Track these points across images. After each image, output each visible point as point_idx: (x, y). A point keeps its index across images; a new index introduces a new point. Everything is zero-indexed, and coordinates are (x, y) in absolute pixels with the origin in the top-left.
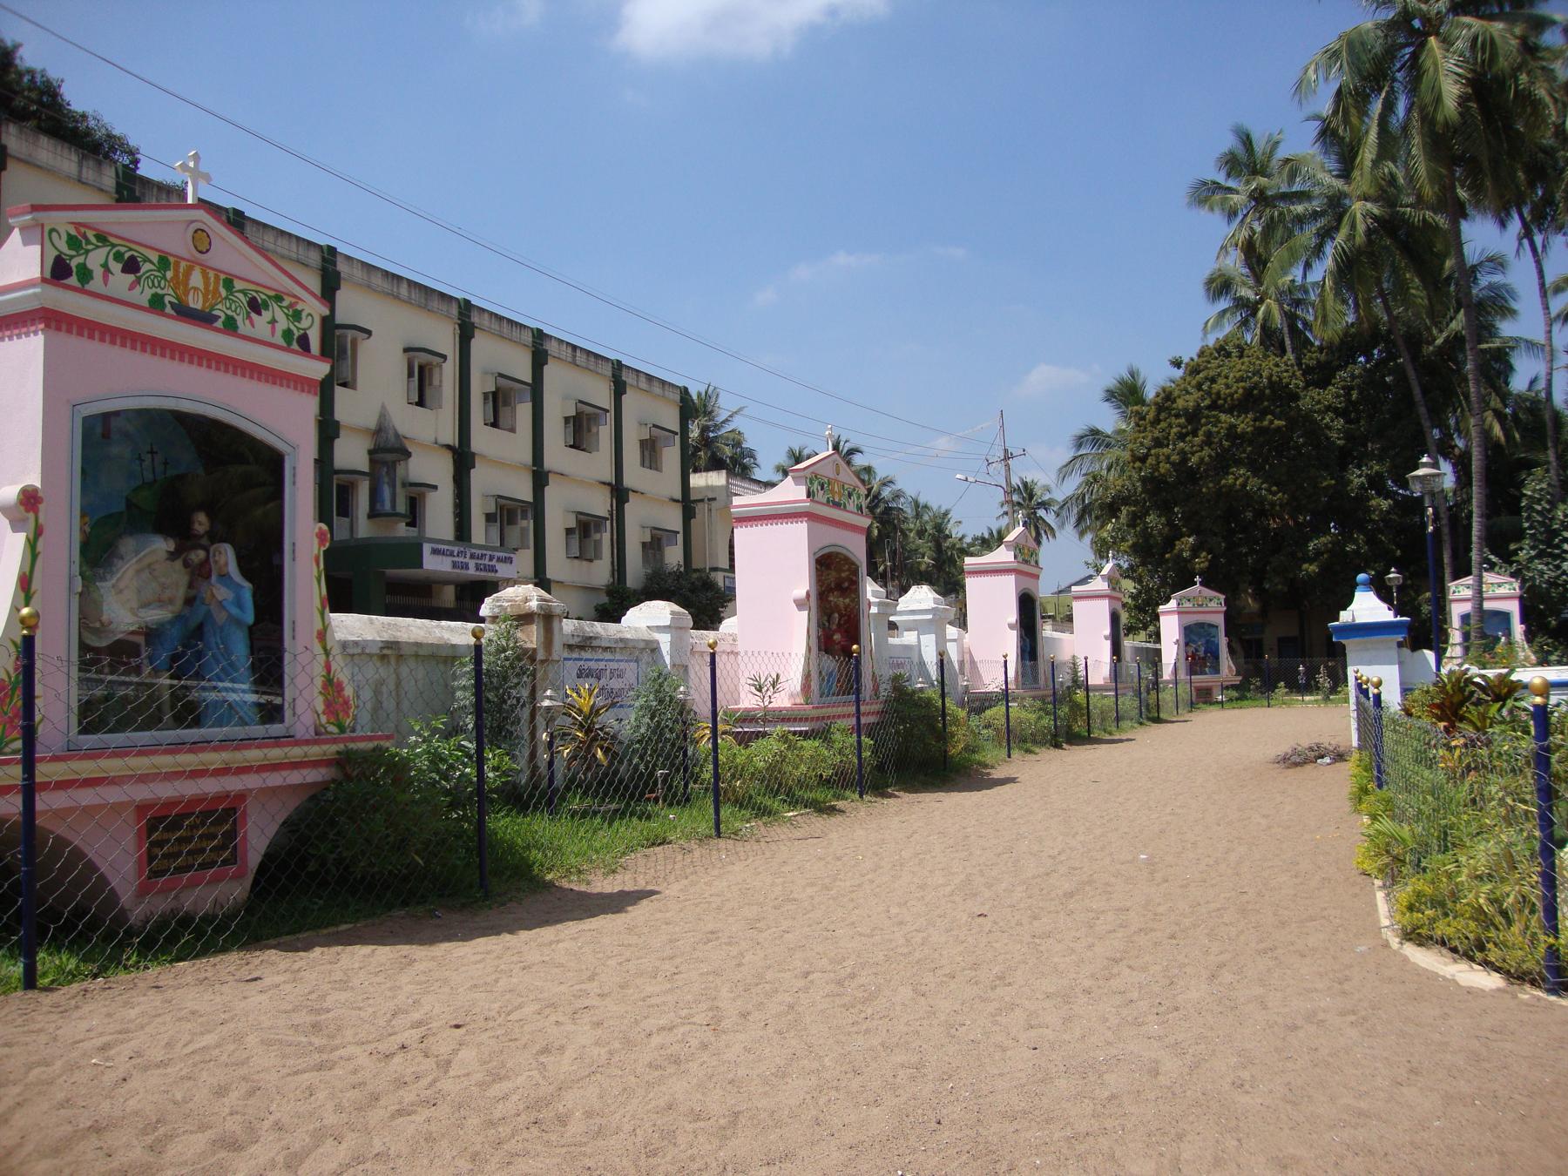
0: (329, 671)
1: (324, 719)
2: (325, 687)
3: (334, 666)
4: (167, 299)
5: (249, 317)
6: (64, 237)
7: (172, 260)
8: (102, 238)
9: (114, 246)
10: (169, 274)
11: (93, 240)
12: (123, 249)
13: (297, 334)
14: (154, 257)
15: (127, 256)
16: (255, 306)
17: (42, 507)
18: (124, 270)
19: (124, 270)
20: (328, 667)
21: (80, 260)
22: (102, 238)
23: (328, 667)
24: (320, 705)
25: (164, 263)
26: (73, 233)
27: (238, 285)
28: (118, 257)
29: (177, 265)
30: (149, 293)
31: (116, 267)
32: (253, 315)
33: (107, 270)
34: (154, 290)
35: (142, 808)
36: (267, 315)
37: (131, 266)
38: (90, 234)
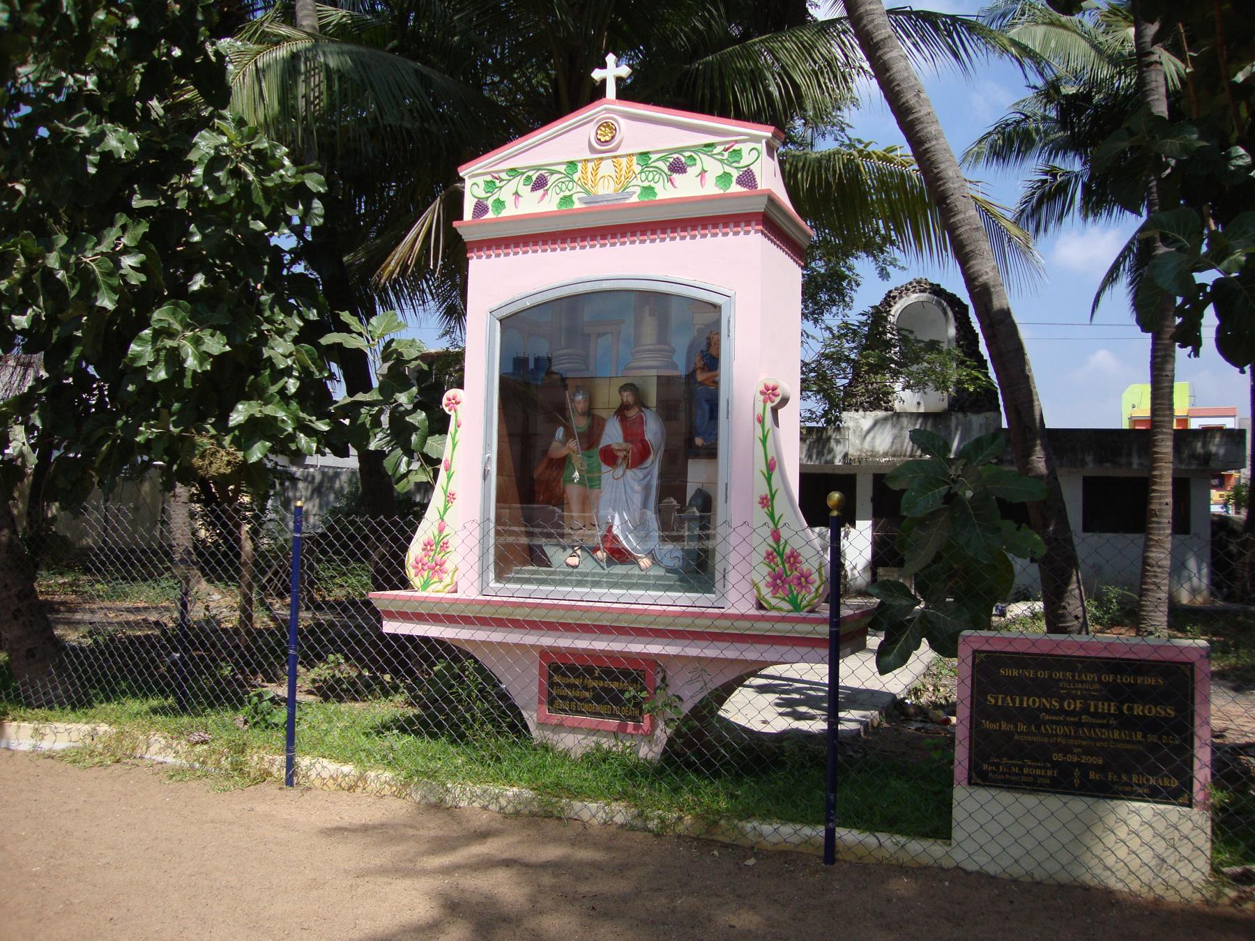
1: (766, 592)
2: (770, 557)
3: (784, 533)
4: (575, 198)
5: (670, 180)
6: (482, 185)
8: (514, 172)
10: (576, 177)
12: (530, 173)
13: (735, 174)
15: (534, 178)
16: (677, 168)
19: (534, 189)
20: (776, 536)
21: (495, 197)
23: (776, 536)
24: (762, 574)
30: (556, 199)
31: (525, 190)
32: (675, 176)
34: (562, 195)
35: (545, 653)
36: (692, 171)
37: (540, 184)
38: (504, 176)
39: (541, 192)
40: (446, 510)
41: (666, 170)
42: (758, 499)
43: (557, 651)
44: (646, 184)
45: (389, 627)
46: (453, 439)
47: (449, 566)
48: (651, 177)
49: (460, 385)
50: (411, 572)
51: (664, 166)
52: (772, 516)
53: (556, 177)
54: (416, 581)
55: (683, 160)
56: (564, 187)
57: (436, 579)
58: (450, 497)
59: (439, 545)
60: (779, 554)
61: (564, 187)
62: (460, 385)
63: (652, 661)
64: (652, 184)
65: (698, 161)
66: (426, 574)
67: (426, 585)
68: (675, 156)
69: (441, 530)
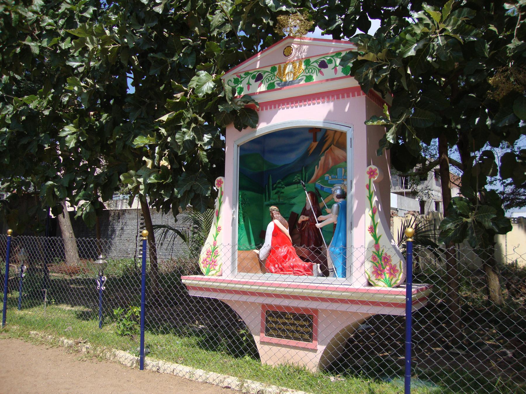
0: (378, 250)
7: (277, 66)
8: (247, 74)
9: (252, 74)
10: (276, 73)
11: (243, 76)
12: (255, 73)
14: (269, 69)
17: (223, 185)
18: (256, 81)
19: (256, 81)
22: (247, 74)
25: (274, 69)
26: (236, 77)
27: (312, 60)
28: (253, 78)
29: (280, 67)
31: (252, 81)
32: (322, 70)
33: (249, 84)
34: (269, 82)
35: (263, 306)
36: (331, 66)
38: (242, 75)
39: (260, 82)
40: (217, 235)
41: (318, 67)
42: (367, 229)
43: (270, 306)
44: (308, 74)
45: (192, 293)
46: (220, 200)
47: (219, 263)
48: (310, 71)
49: (223, 175)
50: (201, 266)
51: (316, 65)
52: (374, 236)
53: (267, 74)
54: (203, 270)
55: (326, 61)
56: (270, 79)
57: (212, 269)
58: (219, 229)
59: (214, 252)
60: (378, 255)
61: (270, 79)
62: (223, 175)
63: (316, 311)
64: (311, 74)
65: (333, 61)
66: (208, 266)
67: (209, 271)
68: (322, 59)
69: (215, 244)
